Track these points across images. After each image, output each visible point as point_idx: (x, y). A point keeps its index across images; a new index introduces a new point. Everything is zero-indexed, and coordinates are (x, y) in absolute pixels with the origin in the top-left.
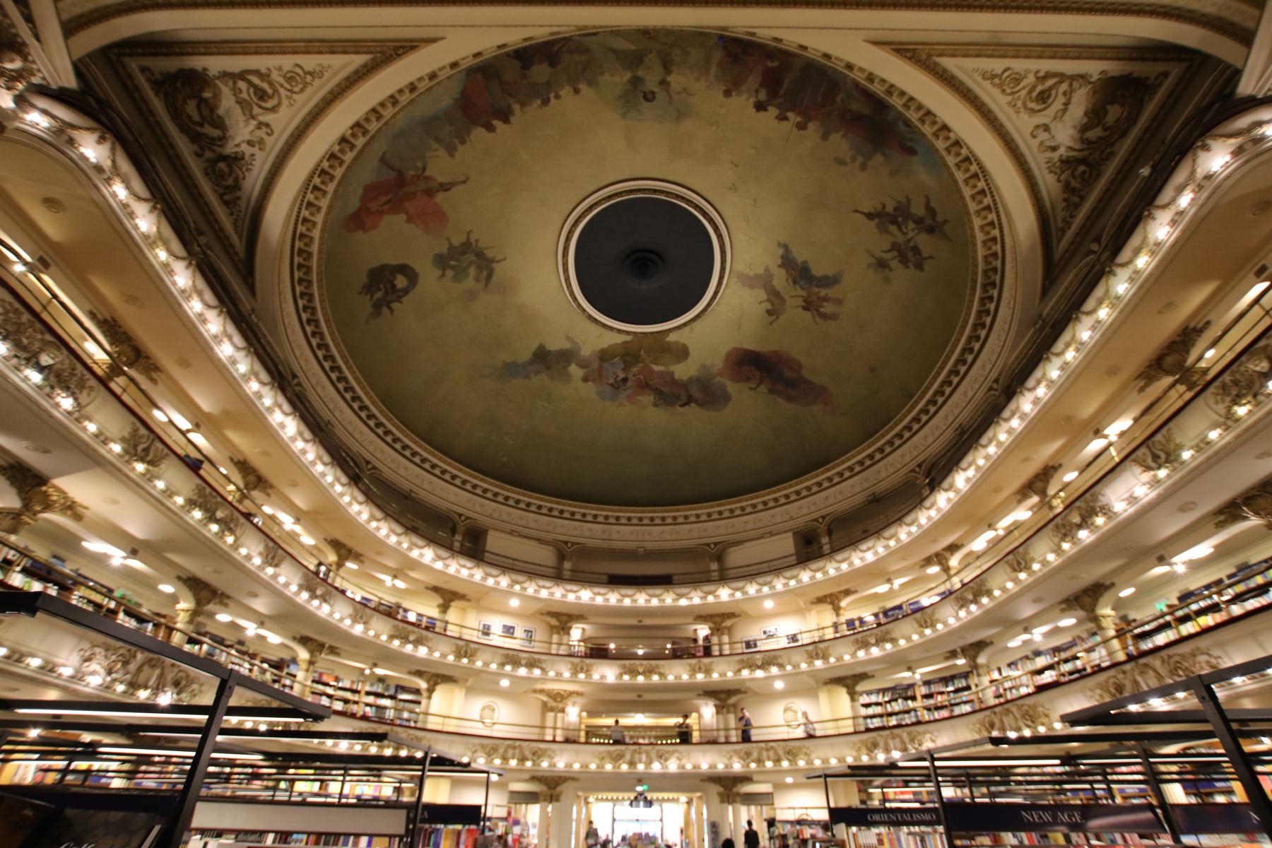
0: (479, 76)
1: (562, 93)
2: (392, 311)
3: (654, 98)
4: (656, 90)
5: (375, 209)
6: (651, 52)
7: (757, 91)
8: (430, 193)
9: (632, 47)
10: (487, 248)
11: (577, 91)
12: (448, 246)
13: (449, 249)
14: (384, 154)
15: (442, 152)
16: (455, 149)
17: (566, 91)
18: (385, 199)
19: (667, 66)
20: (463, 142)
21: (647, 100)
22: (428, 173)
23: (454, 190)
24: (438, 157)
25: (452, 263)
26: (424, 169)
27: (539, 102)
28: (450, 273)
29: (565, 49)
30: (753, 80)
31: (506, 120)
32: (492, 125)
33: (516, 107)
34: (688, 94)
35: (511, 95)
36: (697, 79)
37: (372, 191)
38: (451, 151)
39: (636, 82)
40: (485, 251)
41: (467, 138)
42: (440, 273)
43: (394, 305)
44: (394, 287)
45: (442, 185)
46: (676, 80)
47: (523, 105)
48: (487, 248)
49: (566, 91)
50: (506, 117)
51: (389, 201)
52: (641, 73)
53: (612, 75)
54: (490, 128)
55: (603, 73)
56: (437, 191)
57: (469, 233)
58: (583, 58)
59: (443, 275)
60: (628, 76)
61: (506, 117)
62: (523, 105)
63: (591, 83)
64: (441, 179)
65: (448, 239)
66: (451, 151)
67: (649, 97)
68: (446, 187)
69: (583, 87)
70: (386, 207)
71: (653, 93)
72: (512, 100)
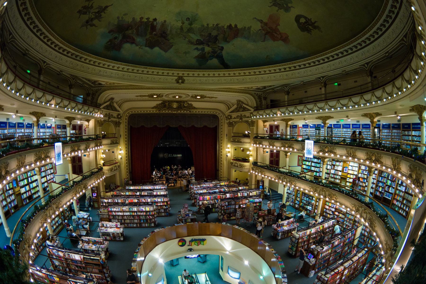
0: (228, 40)
1: (212, 25)
4: (186, 21)
5: (280, 36)
7: (157, 24)
8: (266, 24)
11: (208, 25)
15: (252, 29)
16: (249, 27)
17: (211, 25)
18: (275, 34)
19: (182, 28)
20: (245, 27)
21: (189, 18)
22: (261, 28)
26: (260, 30)
27: (219, 26)
29: (206, 37)
30: (158, 27)
31: (231, 25)
33: (225, 27)
35: (225, 31)
36: (174, 25)
37: (274, 39)
38: (249, 28)
39: (191, 24)
45: (261, 23)
46: (179, 24)
47: (224, 27)
49: (211, 25)
51: (276, 33)
52: (189, 26)
54: (236, 26)
55: (199, 28)
58: (202, 33)
60: (192, 26)
61: (230, 27)
62: (224, 27)
64: (259, 24)
67: (188, 19)
68: (261, 21)
69: (206, 25)
70: (278, 33)
72: (225, 30)
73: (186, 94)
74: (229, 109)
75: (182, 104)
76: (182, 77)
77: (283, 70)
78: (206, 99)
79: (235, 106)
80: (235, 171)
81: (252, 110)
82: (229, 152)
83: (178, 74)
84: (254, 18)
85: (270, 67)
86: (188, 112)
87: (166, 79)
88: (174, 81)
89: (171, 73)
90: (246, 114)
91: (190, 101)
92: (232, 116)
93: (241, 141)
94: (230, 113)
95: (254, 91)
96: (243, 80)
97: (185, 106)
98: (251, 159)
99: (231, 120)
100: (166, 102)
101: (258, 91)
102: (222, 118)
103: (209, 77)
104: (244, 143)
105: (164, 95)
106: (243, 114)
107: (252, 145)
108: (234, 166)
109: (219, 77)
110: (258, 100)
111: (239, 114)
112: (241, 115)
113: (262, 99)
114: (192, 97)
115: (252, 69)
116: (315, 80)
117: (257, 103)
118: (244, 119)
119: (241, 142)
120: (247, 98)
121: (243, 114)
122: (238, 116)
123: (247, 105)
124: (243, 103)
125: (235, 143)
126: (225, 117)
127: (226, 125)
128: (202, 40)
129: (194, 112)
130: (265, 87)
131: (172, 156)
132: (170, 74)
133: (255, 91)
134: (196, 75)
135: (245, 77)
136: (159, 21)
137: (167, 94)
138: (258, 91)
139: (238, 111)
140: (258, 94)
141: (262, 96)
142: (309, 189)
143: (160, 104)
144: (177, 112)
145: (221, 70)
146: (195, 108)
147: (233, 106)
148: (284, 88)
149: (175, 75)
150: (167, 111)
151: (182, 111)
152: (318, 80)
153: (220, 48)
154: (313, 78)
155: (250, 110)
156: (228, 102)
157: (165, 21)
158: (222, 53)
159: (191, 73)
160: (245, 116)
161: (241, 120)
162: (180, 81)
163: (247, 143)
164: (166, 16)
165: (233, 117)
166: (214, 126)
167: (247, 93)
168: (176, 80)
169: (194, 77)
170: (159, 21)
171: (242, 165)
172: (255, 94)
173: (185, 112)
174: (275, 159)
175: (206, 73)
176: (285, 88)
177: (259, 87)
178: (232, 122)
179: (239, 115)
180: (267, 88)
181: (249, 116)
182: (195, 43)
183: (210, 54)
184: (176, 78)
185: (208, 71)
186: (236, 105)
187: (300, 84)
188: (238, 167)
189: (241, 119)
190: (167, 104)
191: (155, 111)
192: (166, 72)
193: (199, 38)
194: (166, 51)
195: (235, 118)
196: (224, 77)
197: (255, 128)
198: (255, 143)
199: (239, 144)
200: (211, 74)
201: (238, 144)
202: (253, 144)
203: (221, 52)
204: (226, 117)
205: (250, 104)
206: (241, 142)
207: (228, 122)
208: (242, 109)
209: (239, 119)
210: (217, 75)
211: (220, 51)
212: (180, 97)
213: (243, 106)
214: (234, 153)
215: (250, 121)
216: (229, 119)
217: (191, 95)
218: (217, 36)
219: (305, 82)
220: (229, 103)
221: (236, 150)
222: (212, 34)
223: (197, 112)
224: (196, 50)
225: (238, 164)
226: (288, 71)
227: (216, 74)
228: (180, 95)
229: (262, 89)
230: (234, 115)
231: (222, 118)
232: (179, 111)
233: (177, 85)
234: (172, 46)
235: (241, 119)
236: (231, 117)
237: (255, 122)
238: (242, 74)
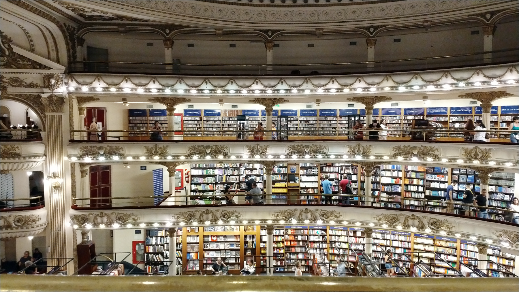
90: (18, 76)
93: (18, 151)
104: (30, 157)
118: (11, 90)
119: (18, 156)
123: (32, 51)
154: (250, 28)
163: (39, 156)
171: (29, 217)
174: (99, 187)
176: (168, 31)
199: (12, 160)
206: (18, 156)
215: (44, 96)
225: (11, 220)
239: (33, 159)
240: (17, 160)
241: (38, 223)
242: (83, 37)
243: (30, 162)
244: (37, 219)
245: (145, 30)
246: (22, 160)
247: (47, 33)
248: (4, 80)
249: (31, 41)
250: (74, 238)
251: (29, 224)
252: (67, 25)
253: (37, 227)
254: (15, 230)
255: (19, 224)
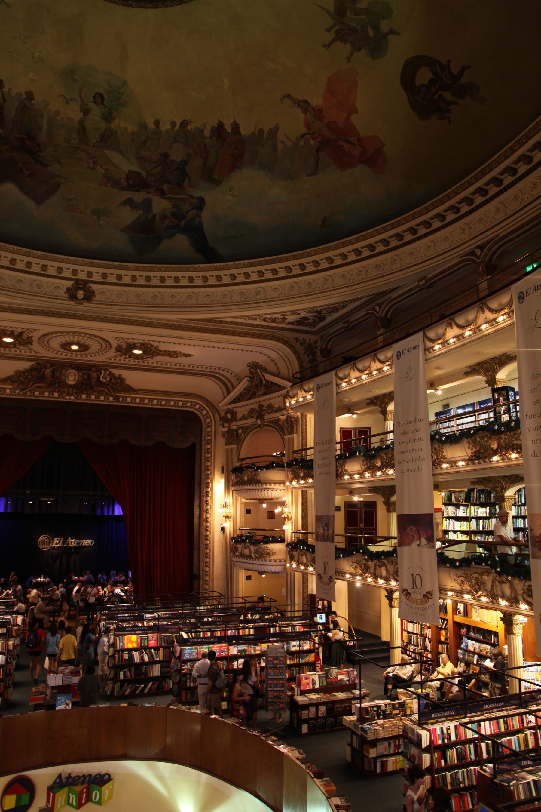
0: (215, 176)
1: (169, 127)
2: (464, 68)
3: (94, 97)
4: (92, 105)
6: (94, 143)
8: (318, 113)
9: (106, 151)
10: (328, 12)
11: (157, 123)
12: (356, 53)
13: (359, 51)
14: (309, 175)
15: (281, 136)
16: (270, 130)
17: (165, 127)
19: (82, 129)
20: (261, 131)
21: (101, 95)
22: (305, 130)
23: (301, 97)
24: (286, 135)
25: (371, 33)
26: (303, 136)
27: (189, 127)
28: (384, 26)
31: (221, 125)
32: (232, 128)
33: (207, 133)
34: (65, 98)
35: (205, 147)
36: (57, 113)
38: (274, 132)
39: (108, 118)
40: (333, 11)
41: (257, 132)
42: (389, 37)
43: (455, 71)
44: (432, 82)
45: (305, 111)
47: (201, 131)
48: (328, 12)
49: (165, 127)
50: (219, 129)
51: (347, 141)
52: (104, 125)
53: (126, 128)
54: (236, 126)
55: (133, 133)
56: (313, 109)
57: (327, 46)
59: (392, 32)
60: (113, 125)
61: (219, 129)
63: (143, 126)
65: (349, 60)
66: (274, 132)
67: (99, 98)
68: (304, 105)
69: (152, 126)
71: (96, 103)
73: (100, 338)
74: (229, 392)
75: (94, 375)
76: (86, 282)
77: (366, 253)
78: (159, 358)
79: (245, 383)
80: (249, 578)
81: (290, 384)
82: (227, 517)
83: (75, 272)
84: (284, 97)
85: (329, 249)
86: (111, 399)
87: (39, 286)
88: (62, 293)
89: (53, 266)
90: (271, 402)
91: (117, 367)
92: (236, 413)
93: (258, 478)
94: (231, 403)
95: (292, 330)
96: (258, 293)
97: (101, 382)
98: (288, 529)
99: (234, 423)
100: (46, 368)
101: (307, 332)
102: (208, 420)
103: (163, 287)
104: (266, 484)
105: (35, 339)
106: (265, 404)
107: (288, 484)
108: (242, 555)
109: (191, 287)
110: (306, 359)
111: (253, 403)
112: (261, 406)
113: (319, 354)
114: (119, 349)
115: (280, 261)
116: (458, 263)
117: (301, 364)
118: (267, 417)
120: (274, 355)
121: (265, 404)
122: (252, 410)
123: (278, 375)
124: (265, 370)
125: (246, 487)
126: (217, 417)
127: (221, 441)
128: (144, 174)
129: (129, 400)
130: (320, 315)
131: (63, 543)
132: (52, 271)
133: (297, 331)
134: (126, 280)
135: (262, 285)
136: (10, 90)
137: (44, 336)
138: (307, 332)
139: (253, 396)
140: (304, 340)
141: (316, 347)
142: (457, 587)
143: (26, 371)
144: (76, 399)
145: (196, 266)
146: (130, 389)
147: (239, 383)
148: (374, 309)
149: (67, 274)
150: (47, 394)
151: (93, 397)
152: (468, 260)
153: (194, 201)
155: (284, 388)
156: (225, 373)
157: (30, 96)
158: (201, 217)
159: (112, 274)
160: (270, 406)
161: (259, 422)
162: (80, 294)
163: (275, 483)
164: (31, 75)
165: (239, 416)
166: (187, 444)
167: (273, 338)
168: (68, 290)
169: (121, 285)
170: (10, 90)
172: (297, 340)
173: (102, 398)
175: (155, 275)
176: (377, 308)
177: (303, 315)
178: (237, 430)
179: (256, 406)
180: (329, 319)
181: (282, 405)
182: (125, 184)
183: (167, 222)
184: (70, 283)
185: (160, 270)
186: (246, 379)
187: (416, 287)
188: (250, 557)
189: (261, 416)
190: (48, 372)
191: (8, 391)
192: (37, 264)
193: (135, 168)
194: (39, 200)
195: (244, 418)
196: (205, 287)
197: (296, 437)
198: (297, 478)
199: (254, 487)
200: (170, 276)
201: (252, 487)
202: (291, 482)
203: (198, 216)
204: (221, 418)
205: (284, 371)
206: (258, 482)
207: (225, 430)
208: (263, 390)
209: (254, 420)
210: (184, 282)
211: (194, 211)
212: (83, 347)
213: (267, 381)
214: (244, 521)
215: (283, 418)
216: (229, 421)
217: (114, 344)
218: (184, 163)
219: (431, 279)
220: (228, 375)
221: (248, 512)
222: (171, 158)
223: (138, 400)
224: (128, 208)
226: (381, 253)
227: (184, 276)
228: (83, 340)
229: (314, 324)
230: (242, 409)
231: (208, 420)
232: (84, 397)
233: (70, 306)
234: (59, 185)
235: (261, 416)
236: (234, 414)
237: (296, 419)
238: (255, 277)
239: (268, 486)
240: (257, 487)
241: (272, 557)
242: (329, 348)
243: (268, 489)
244: (271, 553)
245: (362, 317)
246: (261, 487)
247: (280, 353)
248: (264, 408)
249: (275, 364)
250: (303, 584)
251: (264, 557)
252: (301, 339)
253: (270, 561)
254: (254, 562)
255: (257, 555)
